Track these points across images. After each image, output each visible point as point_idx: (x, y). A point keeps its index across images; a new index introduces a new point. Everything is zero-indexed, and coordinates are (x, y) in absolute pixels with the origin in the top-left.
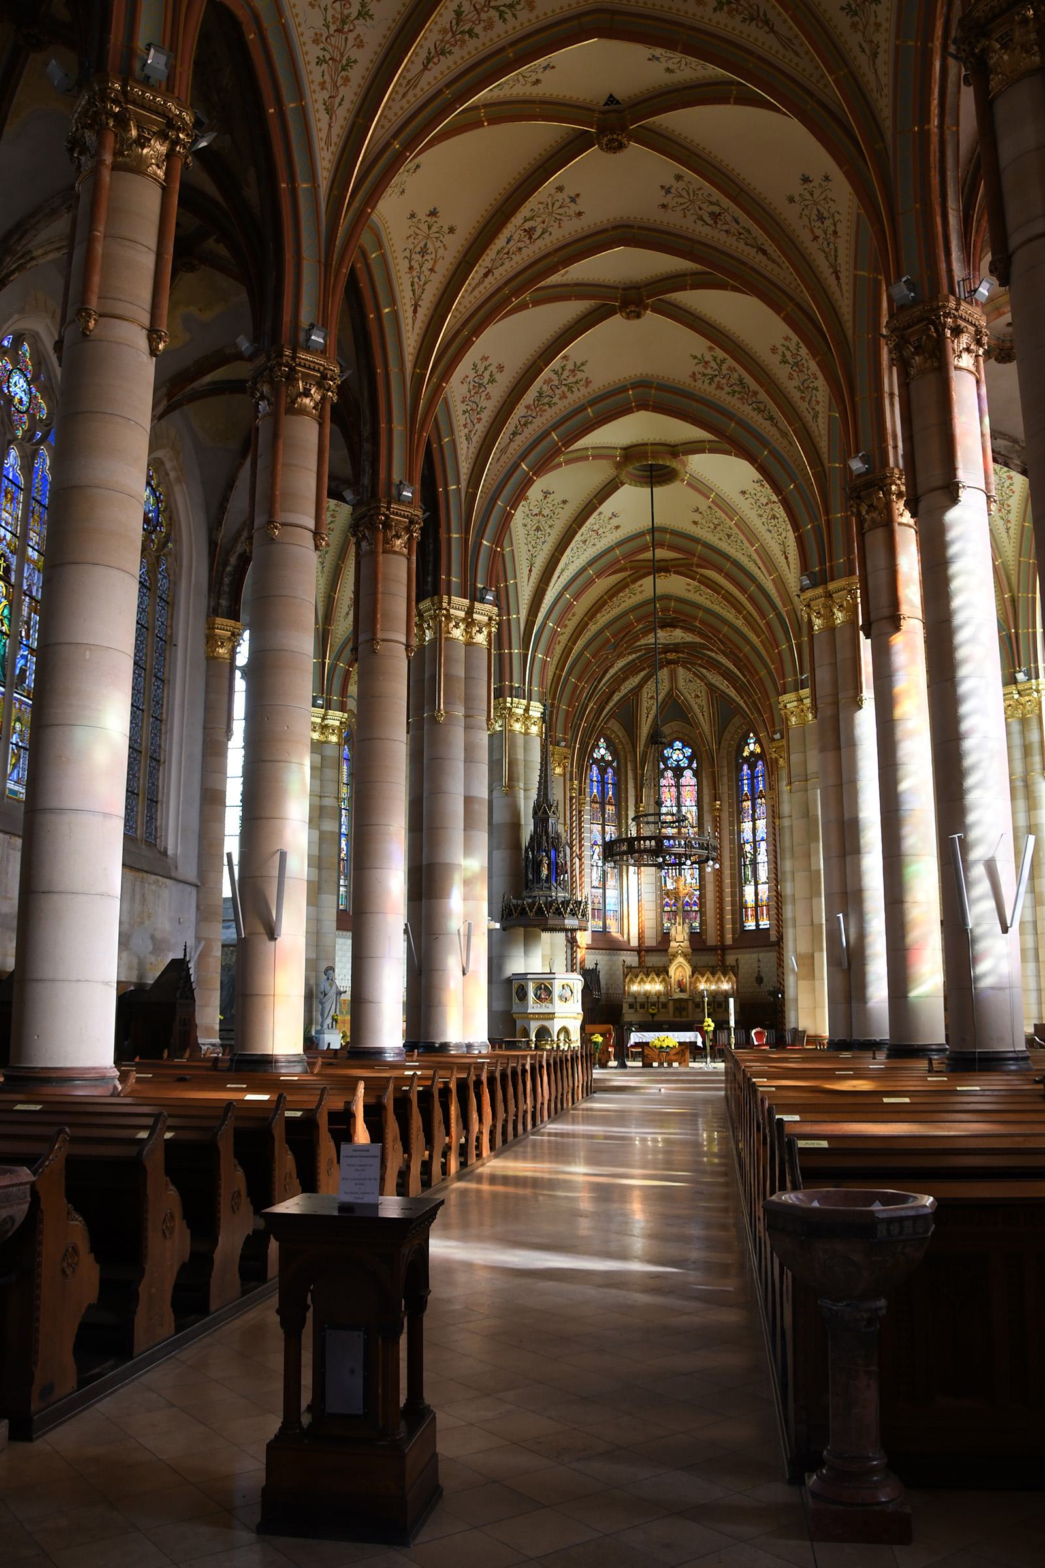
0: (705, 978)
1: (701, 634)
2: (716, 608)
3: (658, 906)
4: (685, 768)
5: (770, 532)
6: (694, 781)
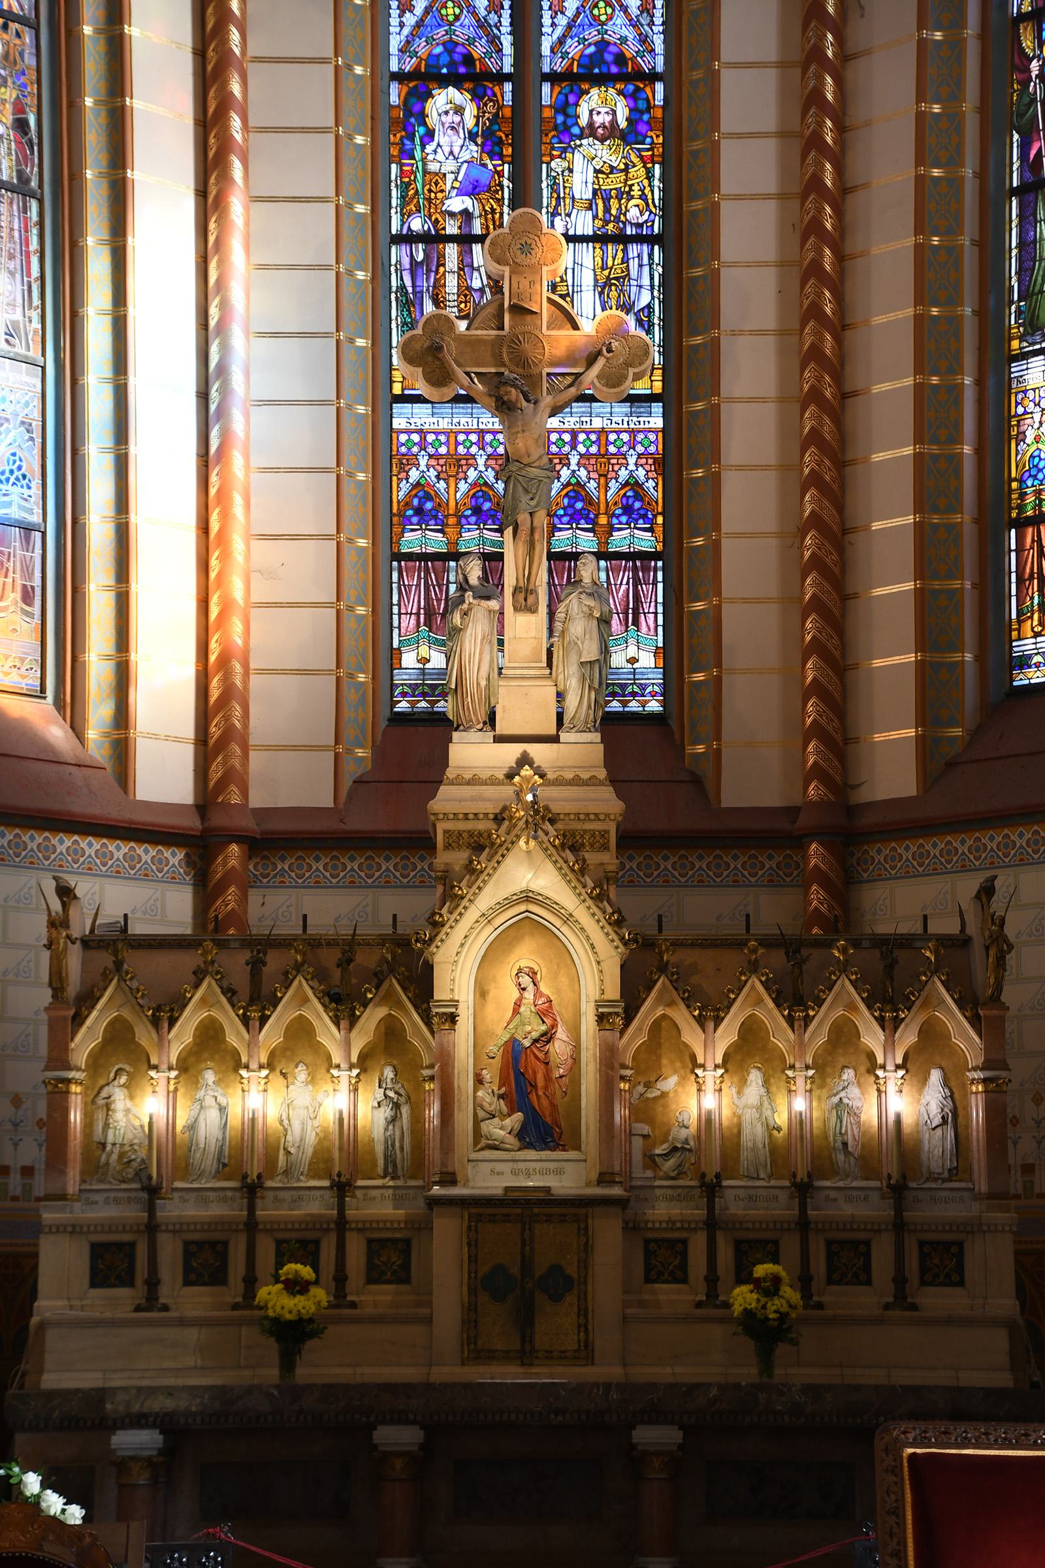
0: (726, 1035)
3: (357, 511)
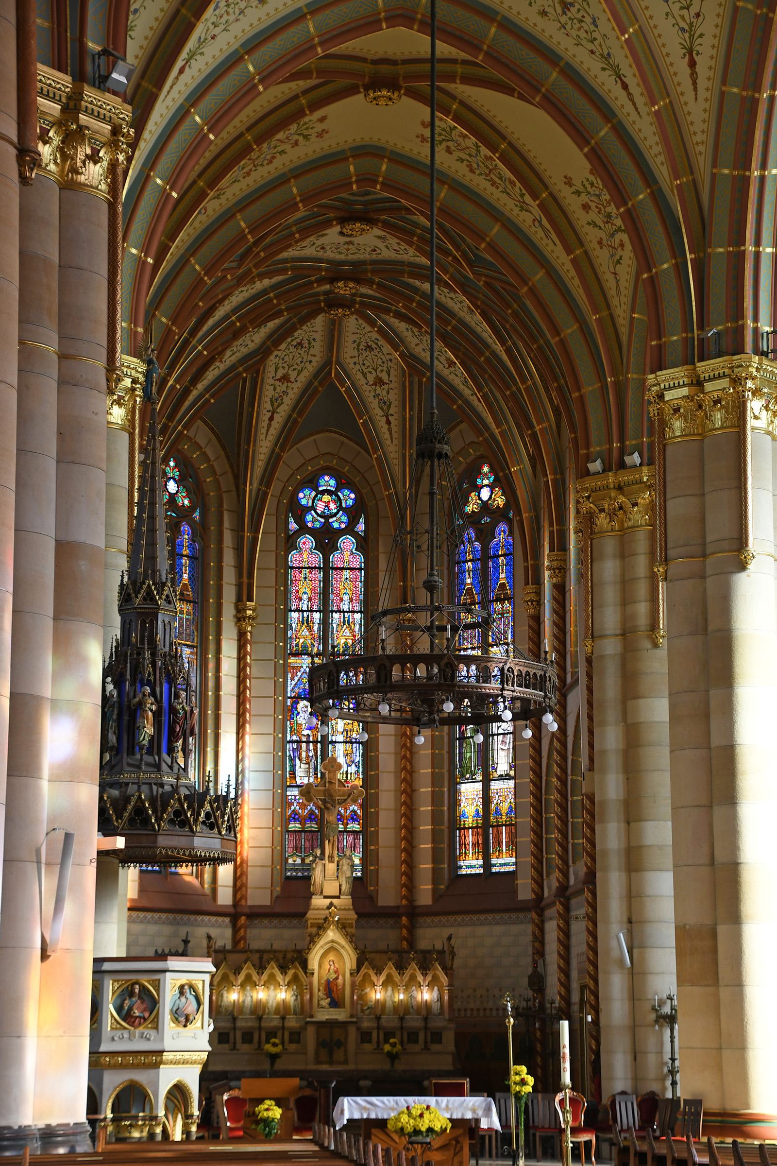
0: (383, 978)
1: (425, 244)
2: (480, 183)
3: (278, 820)
4: (341, 532)
6: (358, 561)
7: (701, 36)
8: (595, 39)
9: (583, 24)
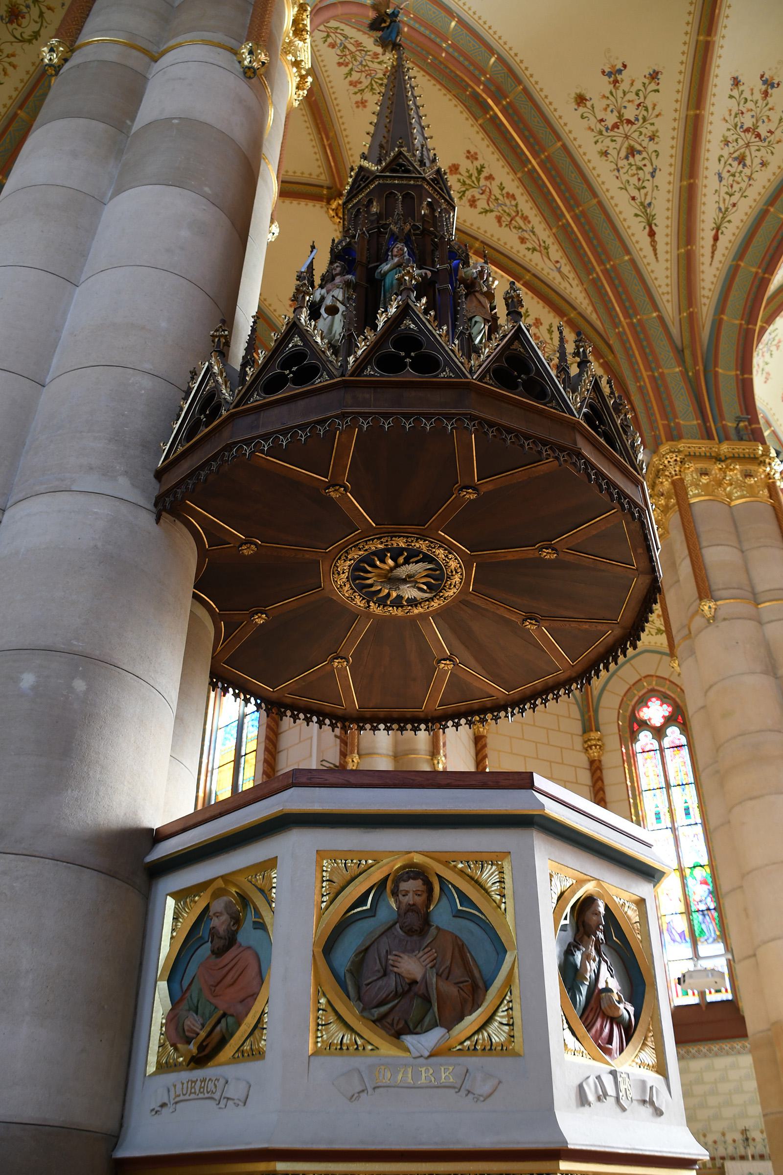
5: (721, 179)
7: (729, 221)
8: (644, 187)
9: (640, 172)
